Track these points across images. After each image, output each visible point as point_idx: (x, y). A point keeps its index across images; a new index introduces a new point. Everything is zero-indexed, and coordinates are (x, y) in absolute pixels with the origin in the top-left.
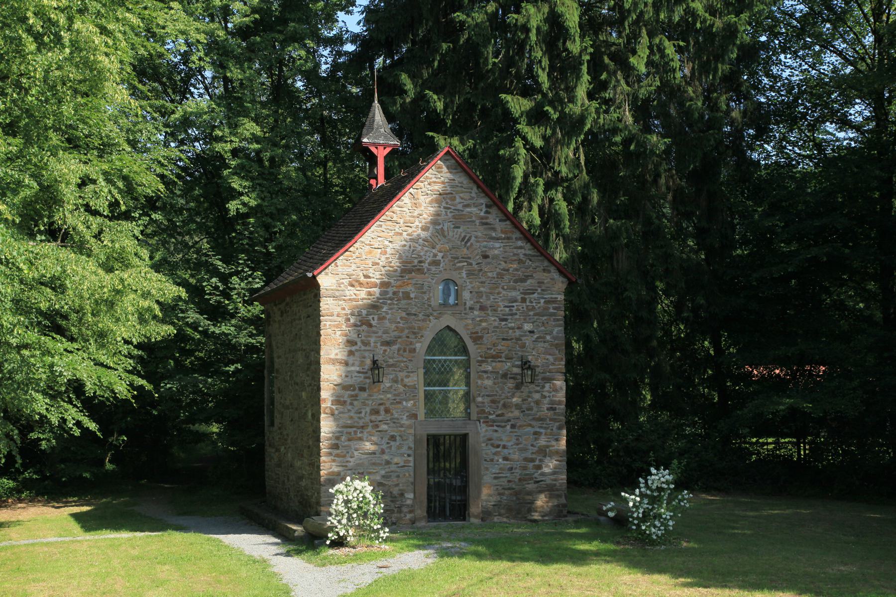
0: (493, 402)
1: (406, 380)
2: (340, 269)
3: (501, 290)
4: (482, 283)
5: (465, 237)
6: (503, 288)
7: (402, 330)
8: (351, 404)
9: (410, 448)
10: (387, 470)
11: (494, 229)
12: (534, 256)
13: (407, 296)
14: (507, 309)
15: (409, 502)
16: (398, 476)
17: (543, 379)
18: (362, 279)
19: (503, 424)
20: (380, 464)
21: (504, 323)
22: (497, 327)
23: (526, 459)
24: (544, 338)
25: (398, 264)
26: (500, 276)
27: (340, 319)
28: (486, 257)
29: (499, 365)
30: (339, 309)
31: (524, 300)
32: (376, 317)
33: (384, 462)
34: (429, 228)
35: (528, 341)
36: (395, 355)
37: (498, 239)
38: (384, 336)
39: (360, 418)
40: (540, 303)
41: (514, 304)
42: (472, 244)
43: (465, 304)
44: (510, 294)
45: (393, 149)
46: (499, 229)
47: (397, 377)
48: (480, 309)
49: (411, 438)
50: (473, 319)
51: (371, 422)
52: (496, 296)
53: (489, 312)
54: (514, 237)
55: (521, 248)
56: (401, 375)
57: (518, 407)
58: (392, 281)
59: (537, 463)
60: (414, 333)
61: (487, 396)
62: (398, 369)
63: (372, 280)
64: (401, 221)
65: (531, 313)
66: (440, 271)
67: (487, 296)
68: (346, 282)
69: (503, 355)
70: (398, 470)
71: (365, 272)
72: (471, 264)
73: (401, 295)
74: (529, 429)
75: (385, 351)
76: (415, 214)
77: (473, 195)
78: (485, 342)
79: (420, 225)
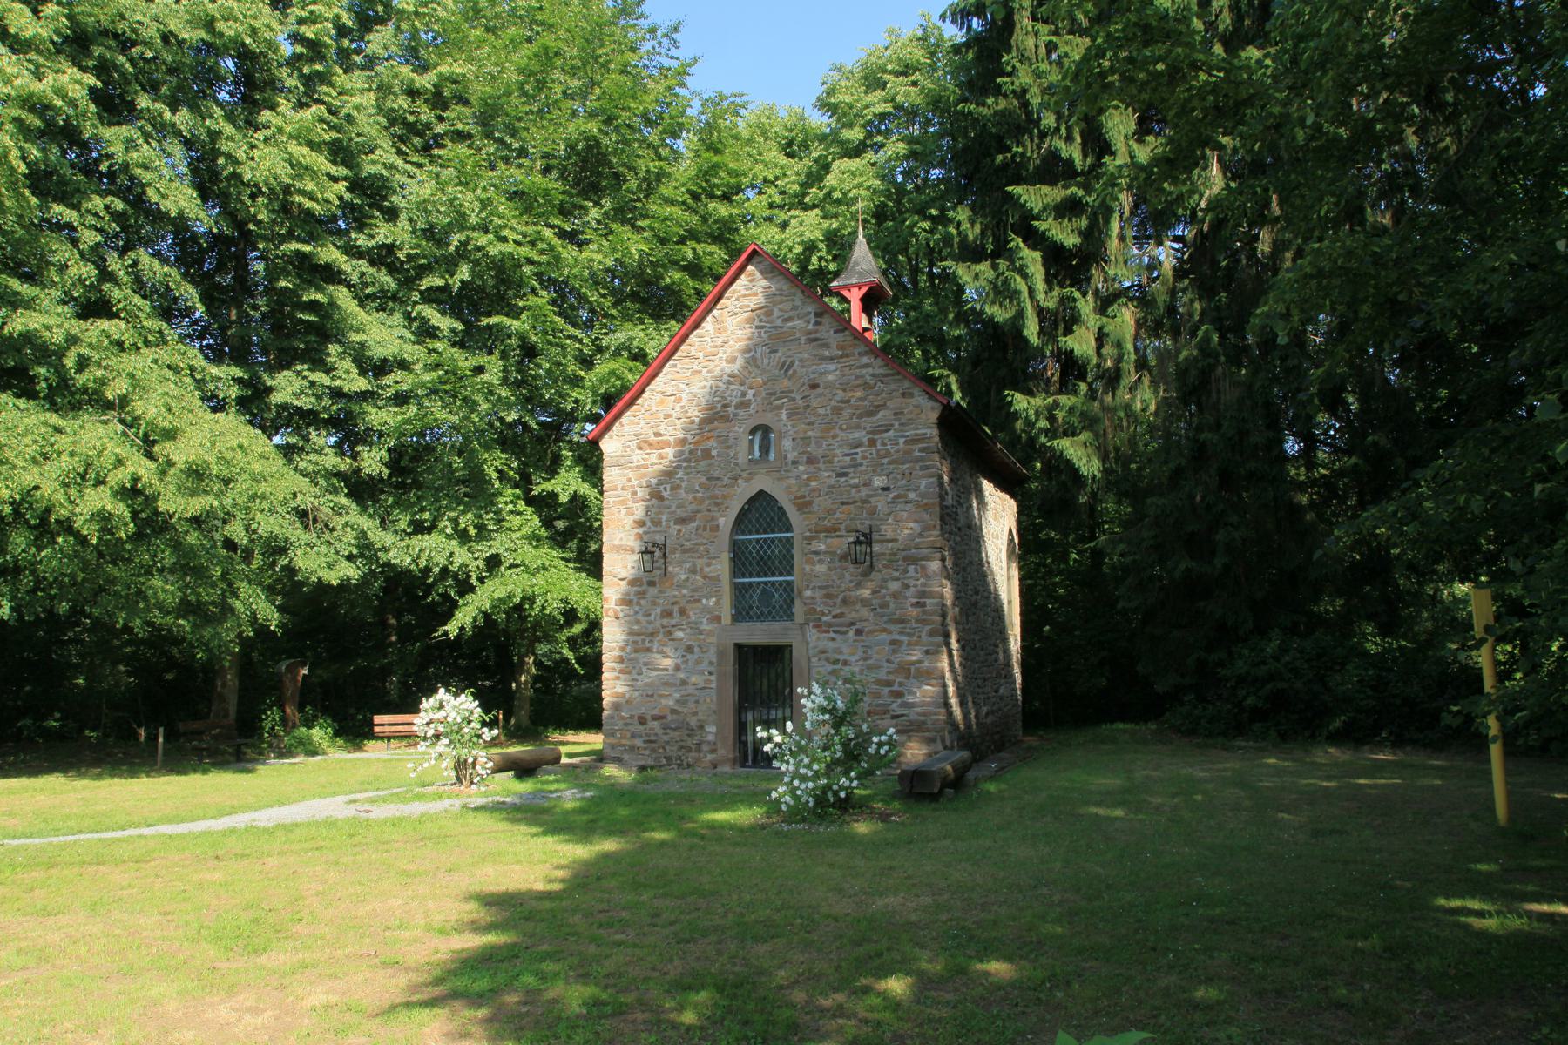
0: (828, 596)
1: (707, 569)
2: (626, 428)
3: (838, 431)
4: (809, 424)
5: (785, 362)
6: (841, 429)
7: (702, 501)
8: (638, 603)
9: (711, 663)
10: (683, 692)
11: (827, 346)
12: (887, 375)
13: (707, 453)
14: (848, 459)
15: (710, 738)
16: (697, 702)
17: (905, 559)
18: (652, 438)
19: (844, 629)
20: (675, 685)
21: (843, 479)
22: (833, 487)
23: (879, 682)
24: (905, 496)
25: (696, 413)
26: (837, 411)
27: (625, 493)
29: (835, 541)
30: (624, 481)
31: (872, 443)
32: (668, 487)
33: (678, 682)
34: (736, 358)
36: (693, 536)
37: (832, 359)
38: (679, 511)
39: (650, 622)
40: (897, 444)
41: (858, 450)
42: (795, 372)
43: (786, 457)
44: (851, 436)
45: (871, 289)
46: (834, 346)
47: (694, 565)
48: (807, 462)
49: (713, 650)
50: (798, 478)
51: (663, 627)
52: (831, 441)
53: (821, 465)
54: (856, 352)
55: (867, 366)
56: (699, 563)
58: (688, 436)
59: (896, 687)
60: (717, 504)
61: (820, 587)
62: (695, 555)
63: (665, 438)
64: (701, 355)
65: (885, 461)
66: (750, 415)
67: (817, 443)
68: (633, 444)
69: (843, 527)
70: (696, 692)
71: (655, 429)
72: (793, 400)
73: (699, 453)
74: (884, 636)
75: (680, 531)
76: (719, 343)
77: (798, 303)
78: (816, 509)
79: (724, 356)
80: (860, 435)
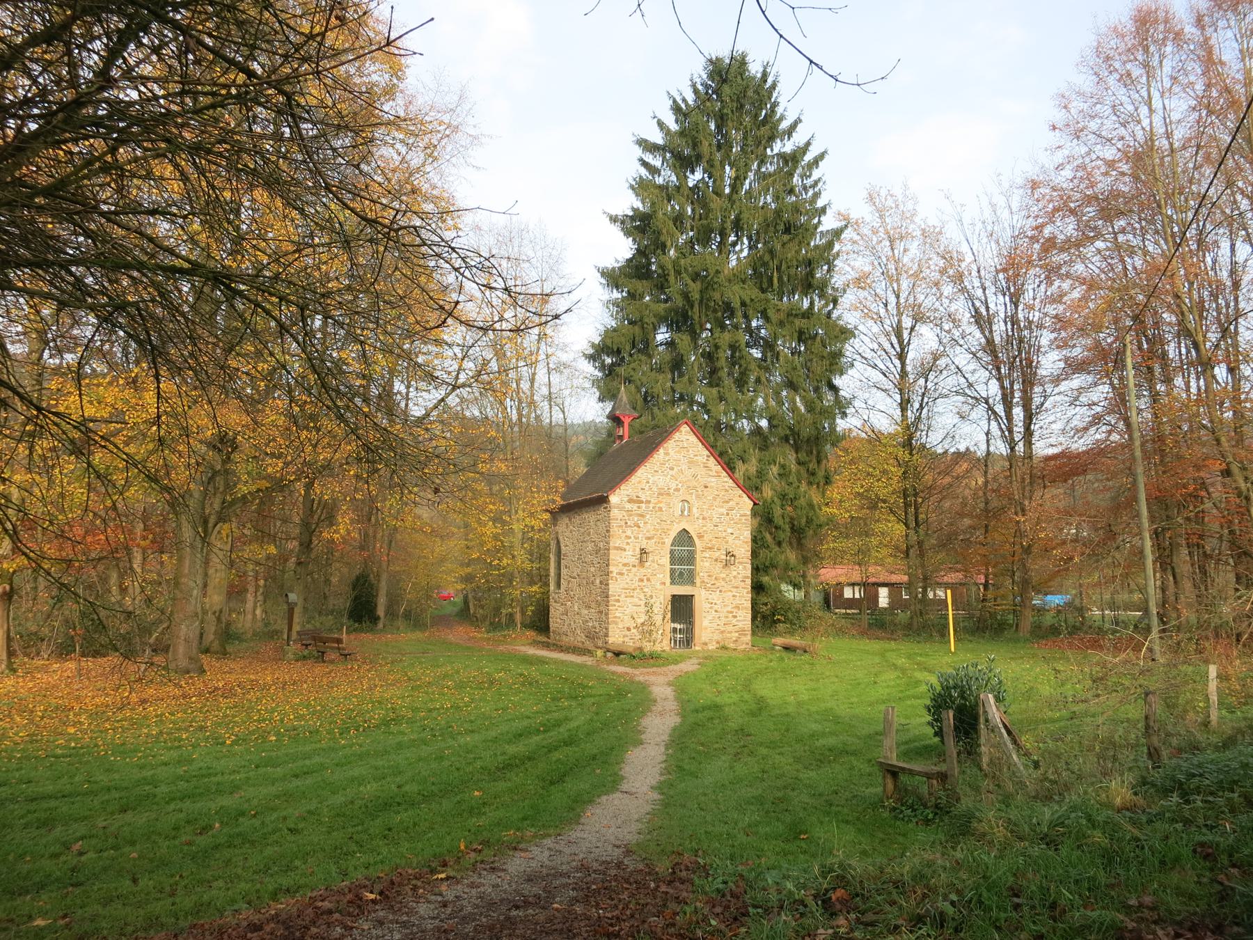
26: (715, 499)
28: (706, 487)
35: (730, 539)
49: (662, 597)
57: (724, 579)
68: (626, 499)
80: (724, 511)
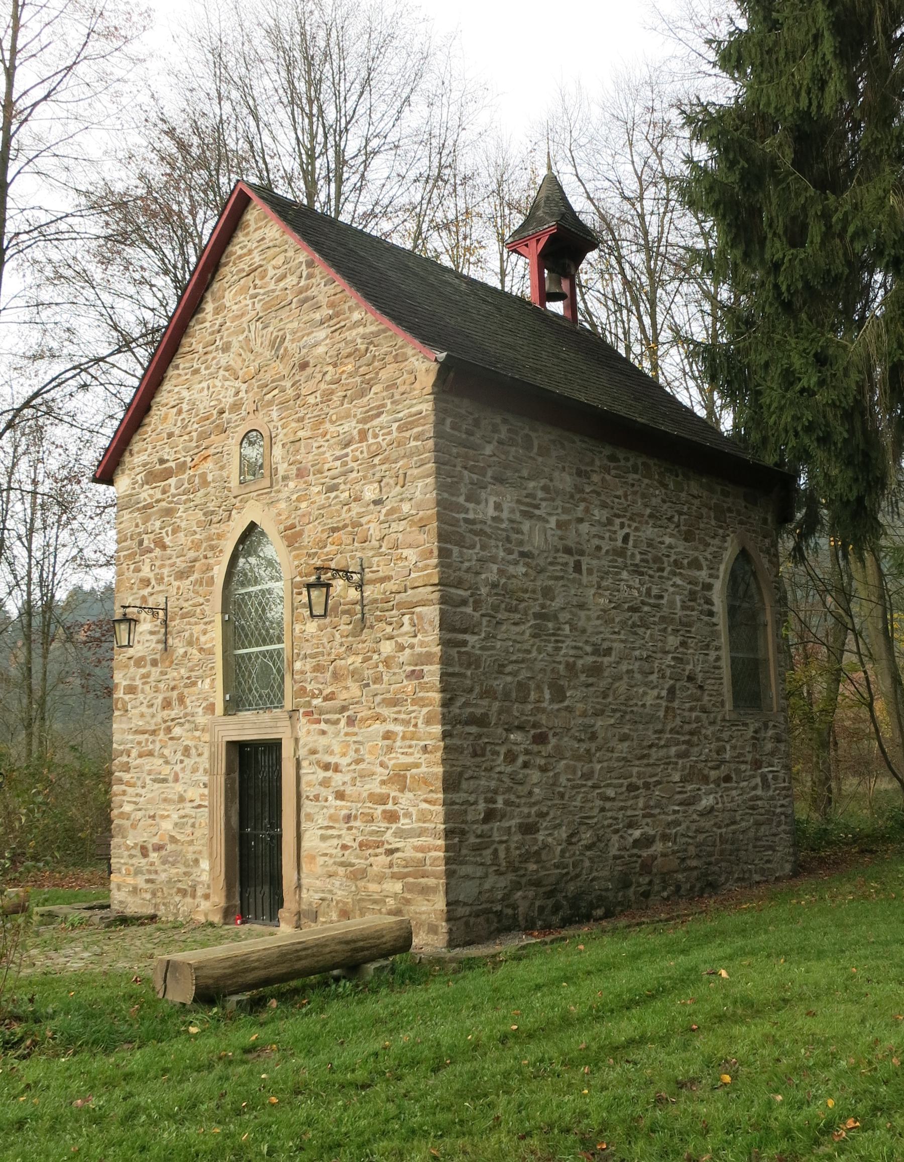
3: (328, 425)
4: (299, 420)
14: (338, 463)
21: (333, 495)
22: (322, 507)
26: (327, 396)
31: (363, 436)
41: (349, 450)
52: (320, 440)
56: (197, 629)
62: (193, 620)
80: (350, 427)
